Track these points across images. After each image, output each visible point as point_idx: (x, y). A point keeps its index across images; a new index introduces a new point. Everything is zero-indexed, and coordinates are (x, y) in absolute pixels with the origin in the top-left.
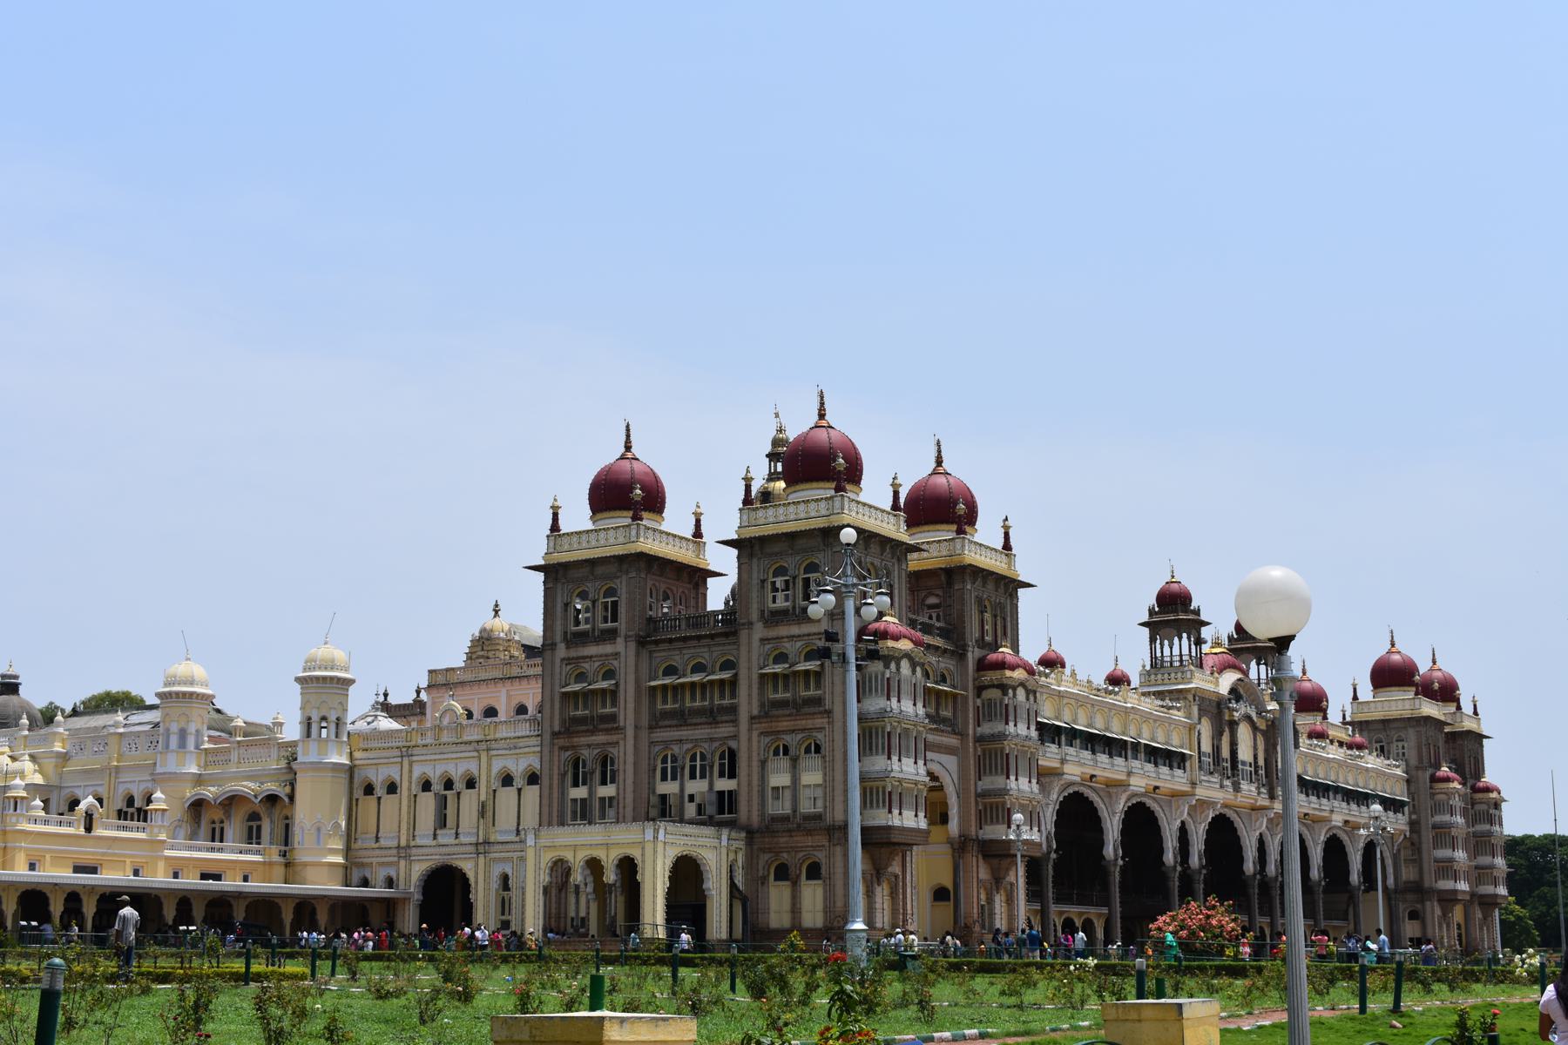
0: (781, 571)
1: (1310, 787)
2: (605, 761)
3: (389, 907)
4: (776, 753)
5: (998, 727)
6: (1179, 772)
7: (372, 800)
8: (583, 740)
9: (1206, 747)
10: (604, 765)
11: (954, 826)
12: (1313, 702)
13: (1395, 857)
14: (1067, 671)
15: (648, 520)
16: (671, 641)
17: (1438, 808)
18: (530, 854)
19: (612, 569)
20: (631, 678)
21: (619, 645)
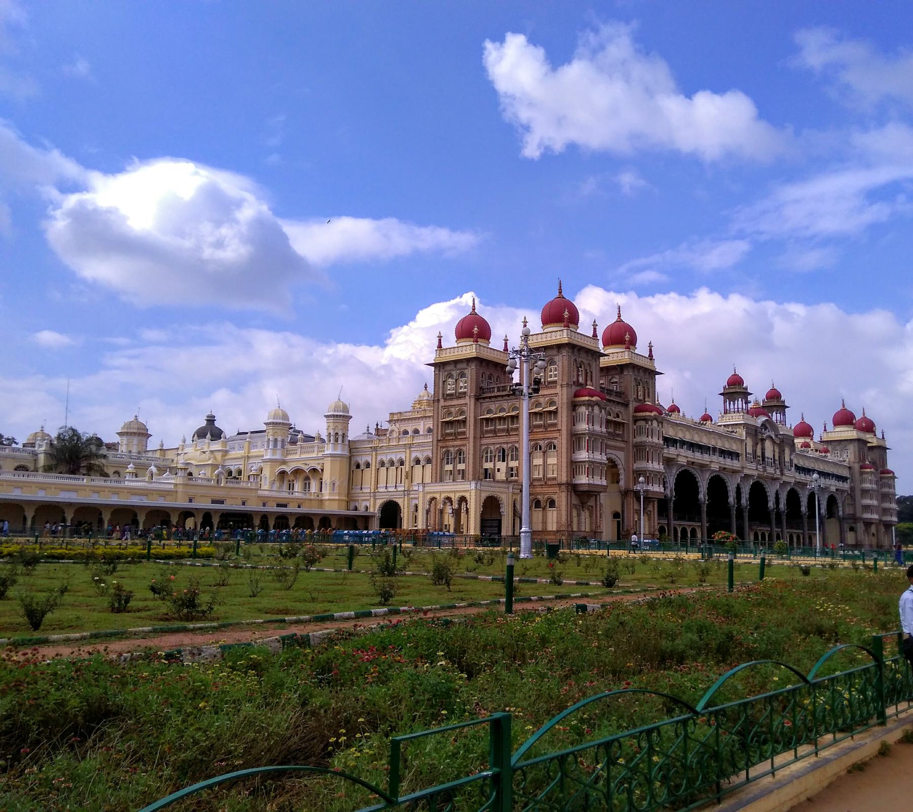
1: (799, 469)
2: (460, 452)
5: (643, 438)
6: (736, 462)
8: (451, 443)
9: (750, 450)
10: (460, 454)
11: (622, 483)
12: (805, 431)
13: (843, 503)
14: (681, 414)
15: (481, 342)
16: (490, 398)
17: (862, 482)
19: (464, 365)
20: (472, 415)
21: (467, 400)
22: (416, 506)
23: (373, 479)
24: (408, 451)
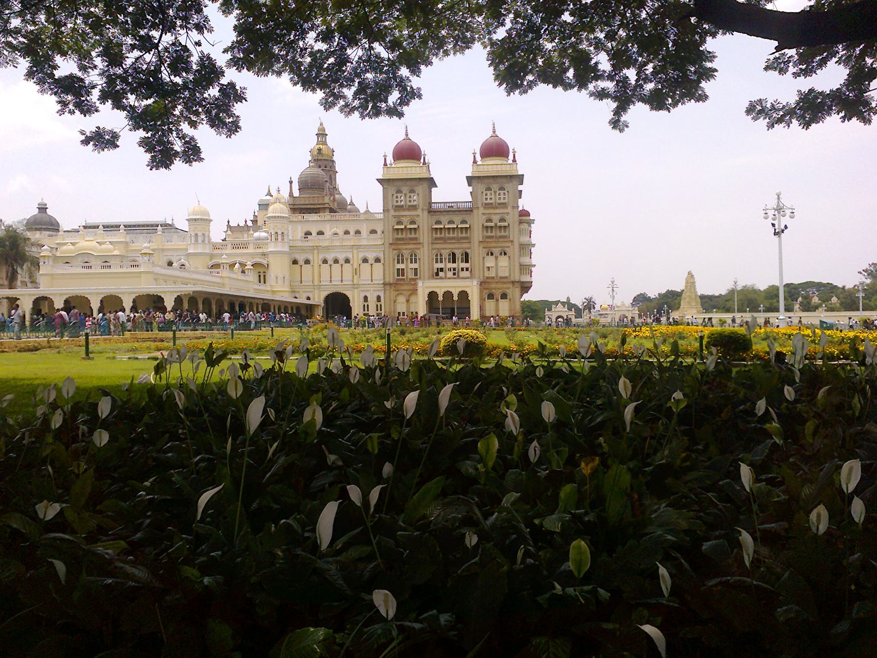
0: (489, 189)
3: (310, 308)
4: (488, 254)
7: (297, 267)
18: (420, 291)
19: (414, 183)
22: (366, 299)
23: (316, 275)
24: (355, 251)
